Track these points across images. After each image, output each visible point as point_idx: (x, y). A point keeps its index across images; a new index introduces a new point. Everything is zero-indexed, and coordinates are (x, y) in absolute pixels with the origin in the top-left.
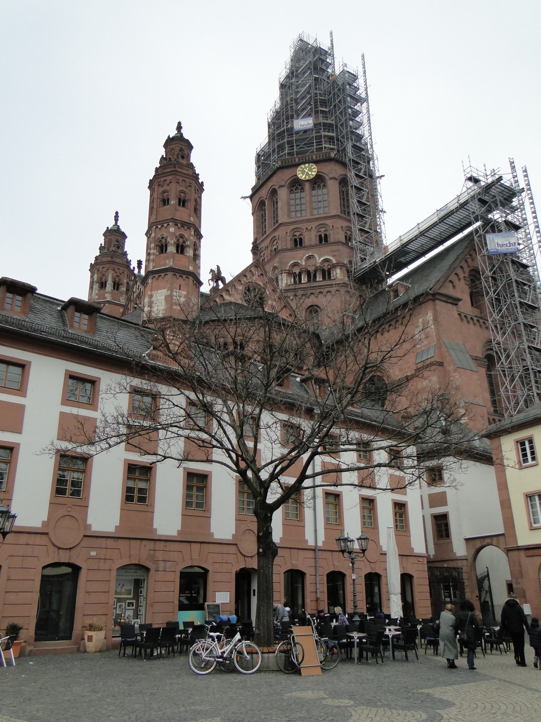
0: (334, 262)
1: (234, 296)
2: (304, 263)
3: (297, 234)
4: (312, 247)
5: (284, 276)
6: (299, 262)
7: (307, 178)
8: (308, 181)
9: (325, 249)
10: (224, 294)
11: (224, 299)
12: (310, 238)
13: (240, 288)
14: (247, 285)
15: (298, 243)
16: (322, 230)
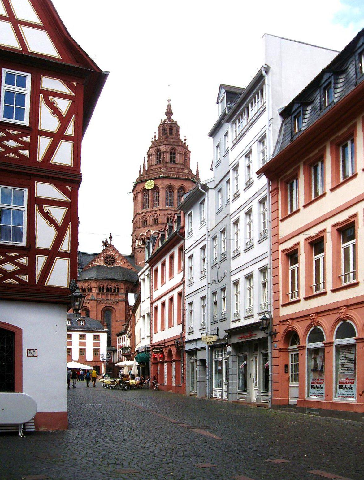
0: (158, 232)
1: (99, 262)
2: (146, 234)
3: (145, 218)
4: (150, 226)
5: (137, 241)
6: (144, 233)
7: (150, 188)
8: (150, 190)
9: (154, 227)
10: (93, 263)
11: (94, 265)
12: (150, 221)
13: (102, 258)
14: (106, 256)
15: (145, 223)
16: (156, 216)
